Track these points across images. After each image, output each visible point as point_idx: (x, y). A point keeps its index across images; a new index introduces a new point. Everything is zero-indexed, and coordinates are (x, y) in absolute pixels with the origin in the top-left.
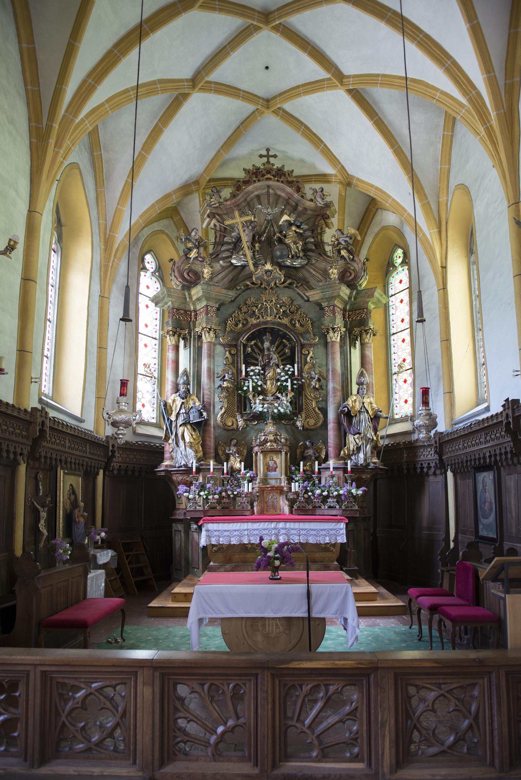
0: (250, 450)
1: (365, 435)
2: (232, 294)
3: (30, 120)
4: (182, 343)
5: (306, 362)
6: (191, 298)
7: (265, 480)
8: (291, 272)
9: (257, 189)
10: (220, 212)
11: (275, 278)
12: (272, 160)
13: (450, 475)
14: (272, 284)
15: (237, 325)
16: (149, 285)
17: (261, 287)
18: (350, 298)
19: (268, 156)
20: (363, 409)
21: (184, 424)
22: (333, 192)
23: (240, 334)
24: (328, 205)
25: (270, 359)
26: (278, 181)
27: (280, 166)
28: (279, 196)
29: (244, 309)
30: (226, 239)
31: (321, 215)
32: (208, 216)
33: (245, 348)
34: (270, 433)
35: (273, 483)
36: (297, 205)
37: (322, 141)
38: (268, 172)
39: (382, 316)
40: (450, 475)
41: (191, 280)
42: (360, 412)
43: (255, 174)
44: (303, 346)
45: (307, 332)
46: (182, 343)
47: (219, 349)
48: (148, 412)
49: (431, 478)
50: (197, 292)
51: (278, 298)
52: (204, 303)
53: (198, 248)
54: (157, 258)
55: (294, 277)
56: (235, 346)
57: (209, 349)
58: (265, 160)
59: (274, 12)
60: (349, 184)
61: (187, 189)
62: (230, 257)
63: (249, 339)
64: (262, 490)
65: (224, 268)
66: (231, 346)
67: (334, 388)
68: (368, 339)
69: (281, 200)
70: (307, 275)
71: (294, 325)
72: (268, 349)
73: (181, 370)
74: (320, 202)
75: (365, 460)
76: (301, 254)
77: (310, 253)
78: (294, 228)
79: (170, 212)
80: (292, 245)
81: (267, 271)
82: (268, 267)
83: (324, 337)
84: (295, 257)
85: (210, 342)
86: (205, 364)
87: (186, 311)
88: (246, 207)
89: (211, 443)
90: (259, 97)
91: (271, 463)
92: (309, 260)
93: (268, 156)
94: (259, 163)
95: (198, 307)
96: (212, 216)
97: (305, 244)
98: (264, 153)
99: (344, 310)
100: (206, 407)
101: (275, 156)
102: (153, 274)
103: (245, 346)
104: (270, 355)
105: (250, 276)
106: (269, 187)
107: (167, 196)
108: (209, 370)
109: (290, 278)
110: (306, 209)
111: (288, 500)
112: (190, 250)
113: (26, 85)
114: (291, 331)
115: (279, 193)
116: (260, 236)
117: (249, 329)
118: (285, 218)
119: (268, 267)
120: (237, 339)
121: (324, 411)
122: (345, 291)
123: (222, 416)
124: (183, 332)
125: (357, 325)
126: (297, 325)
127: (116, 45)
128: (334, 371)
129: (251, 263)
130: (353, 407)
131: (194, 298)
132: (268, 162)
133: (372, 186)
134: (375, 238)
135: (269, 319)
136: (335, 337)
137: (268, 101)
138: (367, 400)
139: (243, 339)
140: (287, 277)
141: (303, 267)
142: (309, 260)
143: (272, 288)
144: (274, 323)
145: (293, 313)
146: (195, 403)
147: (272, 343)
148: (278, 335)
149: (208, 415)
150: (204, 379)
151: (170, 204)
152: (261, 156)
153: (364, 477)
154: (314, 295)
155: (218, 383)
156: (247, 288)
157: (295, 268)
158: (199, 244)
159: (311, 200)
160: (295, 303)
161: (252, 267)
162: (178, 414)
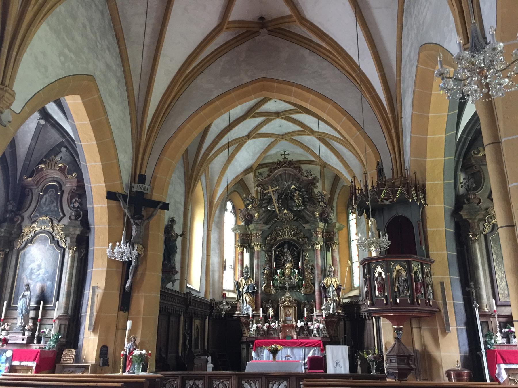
0: (278, 305)
1: (333, 298)
2: (268, 226)
3: (185, 173)
4: (245, 249)
5: (305, 259)
6: (249, 229)
7: (285, 321)
8: (297, 214)
9: (279, 171)
10: (262, 183)
11: (289, 217)
12: (287, 157)
13: (374, 319)
14: (288, 220)
15: (271, 241)
16: (230, 219)
17: (282, 222)
18: (325, 227)
19: (285, 155)
20: (331, 285)
21: (246, 293)
22: (316, 170)
23: (272, 246)
24: (314, 179)
25: (287, 258)
26: (290, 167)
27: (290, 159)
28: (291, 174)
29: (275, 233)
30: (265, 197)
31: (313, 183)
32: (257, 186)
33: (275, 253)
34: (287, 297)
35: (289, 323)
36: (299, 179)
37: (309, 149)
38: (285, 163)
39: (346, 230)
40: (374, 319)
41: (249, 220)
42: (330, 286)
43: (280, 164)
44: (303, 251)
45: (305, 243)
46: (245, 249)
47: (263, 253)
48: (228, 284)
49: (368, 321)
50: (251, 227)
51: (291, 227)
52: (255, 232)
53: (252, 204)
54: (233, 203)
55: (299, 216)
56: (271, 251)
57: (258, 254)
58: (283, 157)
59: (281, 112)
60: (325, 167)
61: (247, 171)
62: (268, 206)
63: (277, 248)
64: (283, 326)
65: (264, 212)
66: (269, 251)
67: (318, 274)
68: (335, 247)
69: (291, 176)
70: (305, 214)
71: (299, 240)
72: (286, 253)
73: (244, 266)
74: (310, 178)
75: (333, 311)
76: (301, 205)
77: (306, 203)
78: (297, 192)
79: (240, 185)
80: (296, 201)
81: (285, 214)
82: (285, 211)
83: (313, 246)
84: (298, 206)
85: (258, 251)
86: (255, 262)
87: (247, 235)
88: (275, 181)
89: (259, 302)
90: (278, 135)
91: (288, 312)
92: (305, 206)
93: (285, 155)
94: (281, 158)
95: (253, 233)
96: (258, 186)
97: (303, 199)
98: (283, 152)
99: (323, 232)
100: (257, 284)
101: (288, 155)
102: (231, 212)
103: (275, 251)
104: (287, 256)
105: (277, 216)
106: (285, 170)
107: (238, 176)
108: (258, 265)
109: (296, 216)
110: (303, 181)
111: (296, 332)
112: (248, 204)
113: (184, 160)
114: (297, 243)
115: (290, 172)
116: (282, 196)
117: (277, 243)
118: (293, 187)
119: (285, 211)
120: (271, 248)
121: (314, 284)
122: (321, 225)
123: (265, 287)
124: (245, 245)
125: (329, 242)
126: (300, 240)
127: (217, 137)
128: (317, 264)
129: (277, 210)
130: (327, 284)
131: (251, 229)
132: (285, 158)
133: (335, 169)
134: (341, 190)
135: (287, 237)
136: (318, 247)
137: (282, 135)
138: (333, 280)
139: (274, 248)
140: (294, 216)
141: (302, 210)
142: (305, 206)
143: (288, 222)
144: (289, 239)
145: (298, 234)
146: (251, 282)
147: (288, 249)
148: (291, 245)
149: (258, 288)
150: (255, 269)
151: (238, 179)
152: (281, 155)
153: (333, 320)
154: (307, 227)
155: (262, 271)
156: (276, 222)
157: (299, 211)
158: (253, 201)
159: (306, 176)
160: (299, 229)
161: (278, 212)
162: (243, 288)
